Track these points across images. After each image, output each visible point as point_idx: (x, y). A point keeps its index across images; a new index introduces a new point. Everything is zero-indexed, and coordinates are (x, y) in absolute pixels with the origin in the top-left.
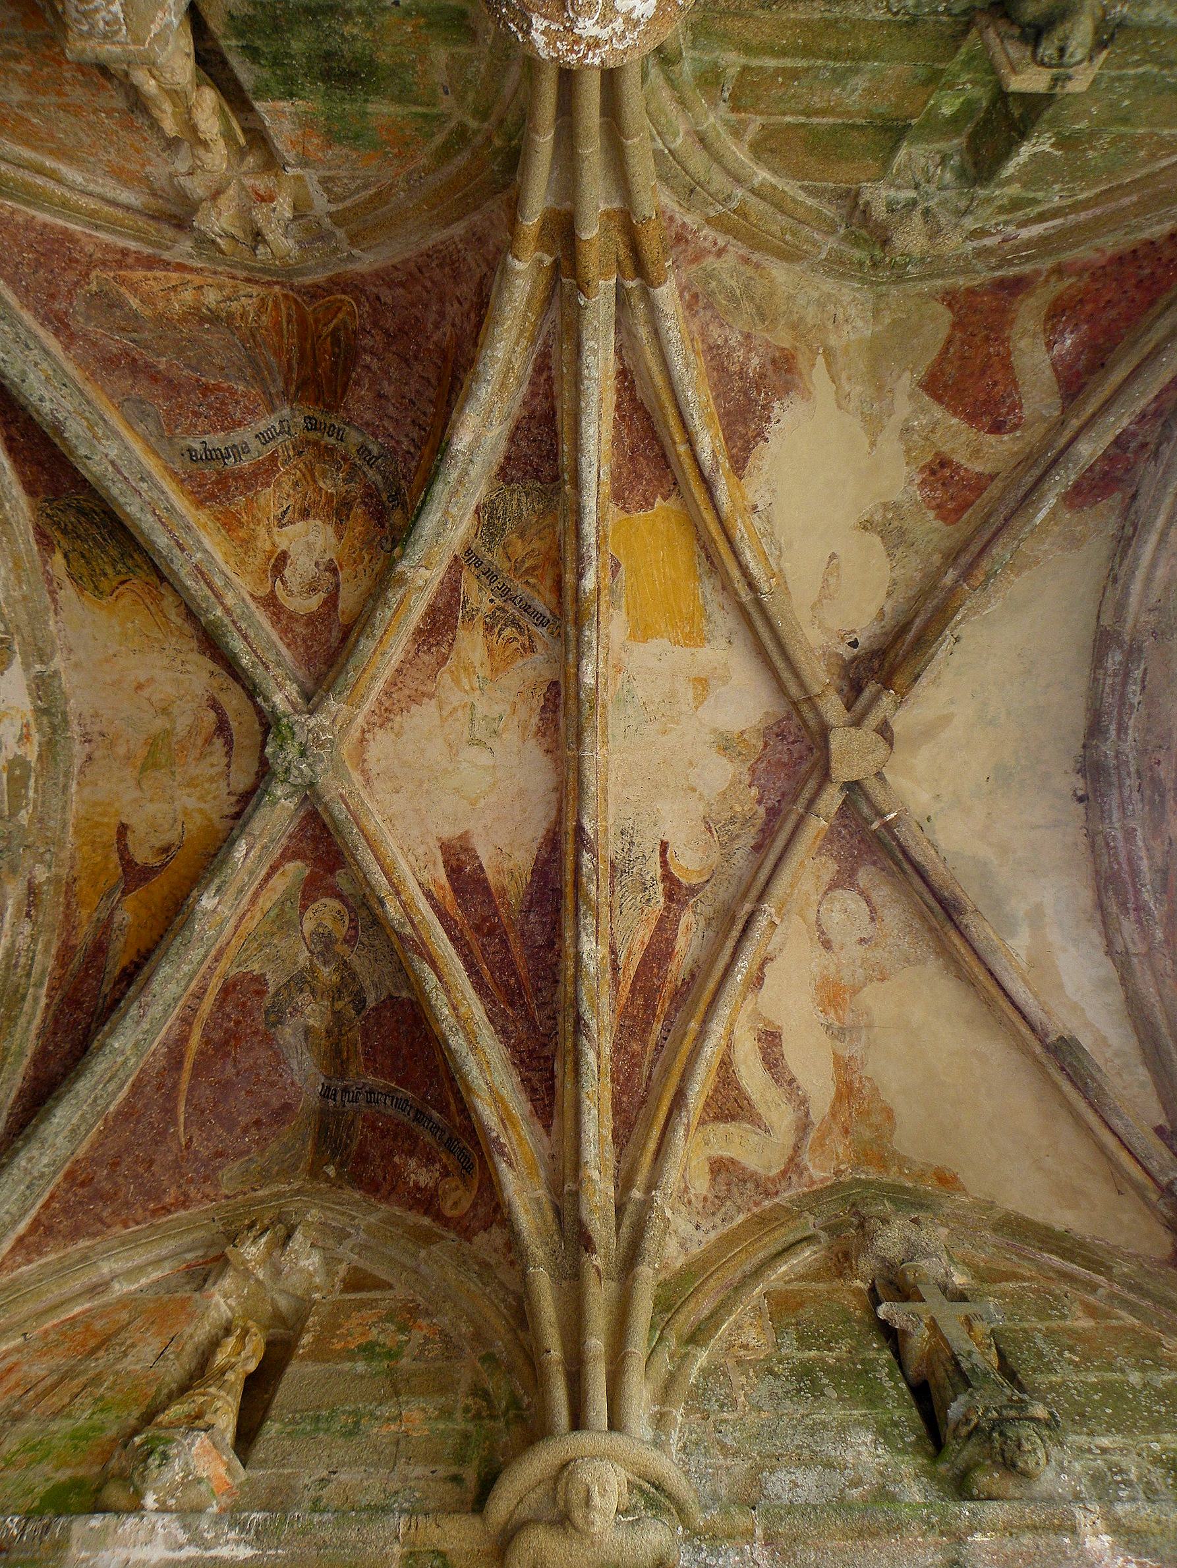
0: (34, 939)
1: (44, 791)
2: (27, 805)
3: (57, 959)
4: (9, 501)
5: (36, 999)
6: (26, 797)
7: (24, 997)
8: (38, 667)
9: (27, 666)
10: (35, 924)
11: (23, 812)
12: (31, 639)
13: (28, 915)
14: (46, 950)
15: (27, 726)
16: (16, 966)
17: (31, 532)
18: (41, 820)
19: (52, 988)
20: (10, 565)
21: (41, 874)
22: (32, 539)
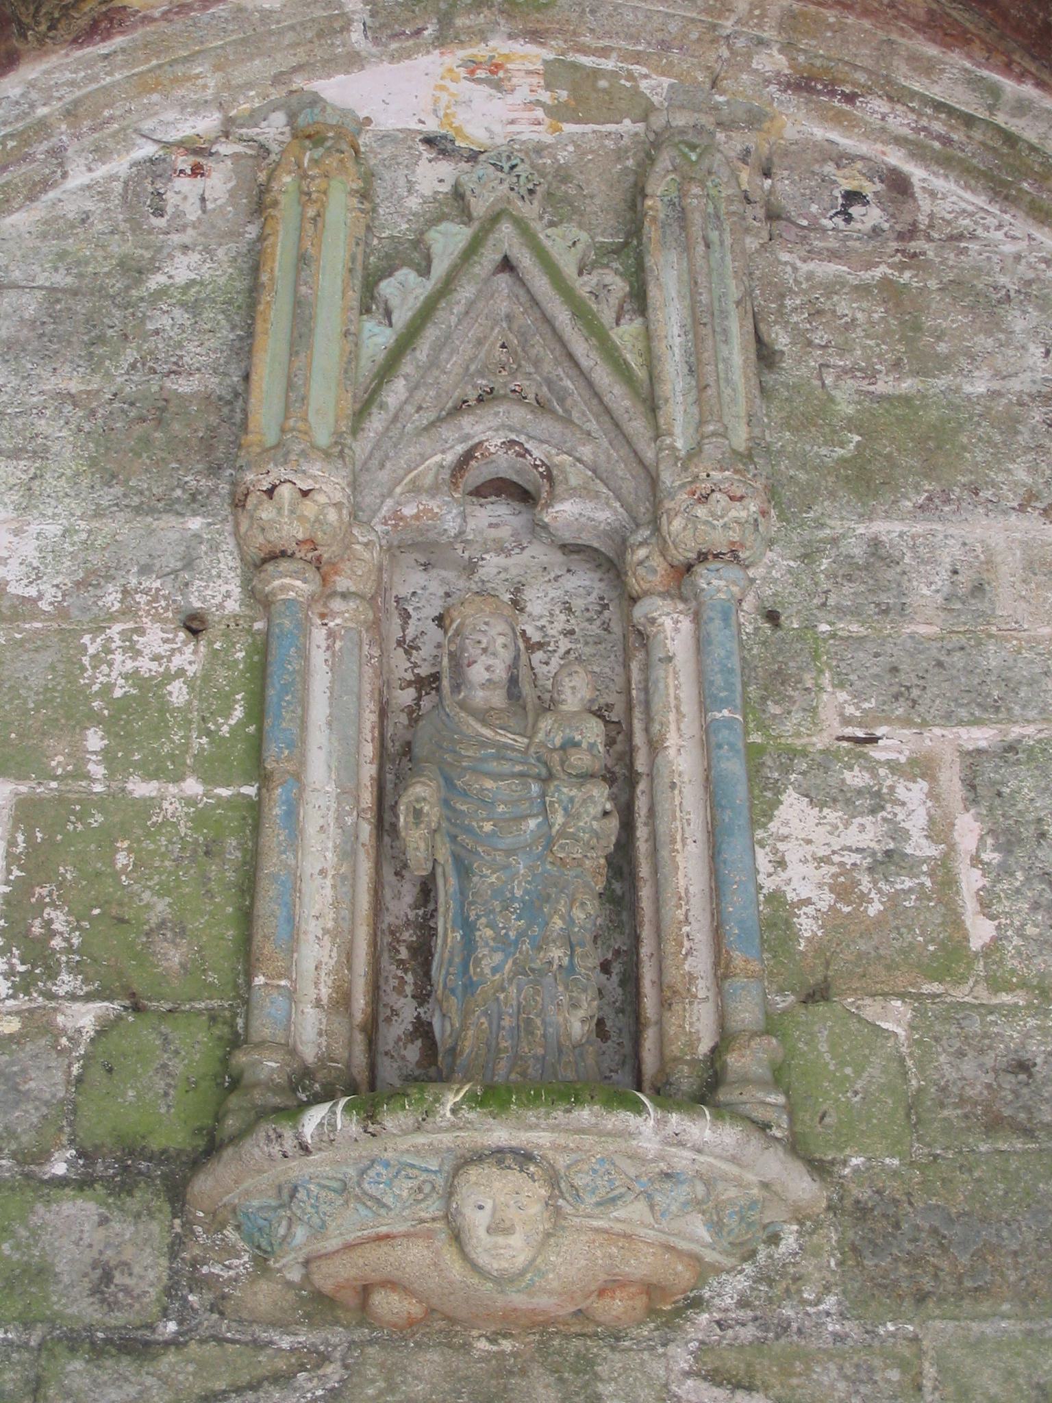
0: (898, 95)
1: (608, 34)
2: (630, 76)
3: (949, 47)
4: (32, 106)
5: (1022, 108)
6: (614, 75)
7: (1011, 139)
8: (356, 36)
9: (354, 61)
10: (870, 91)
11: (644, 85)
12: (300, 50)
13: (850, 98)
14: (928, 68)
15: (472, 66)
16: (946, 141)
17: (89, 51)
18: (665, 46)
19: (1007, 68)
20: (155, 97)
21: (773, 61)
22: (104, 48)
